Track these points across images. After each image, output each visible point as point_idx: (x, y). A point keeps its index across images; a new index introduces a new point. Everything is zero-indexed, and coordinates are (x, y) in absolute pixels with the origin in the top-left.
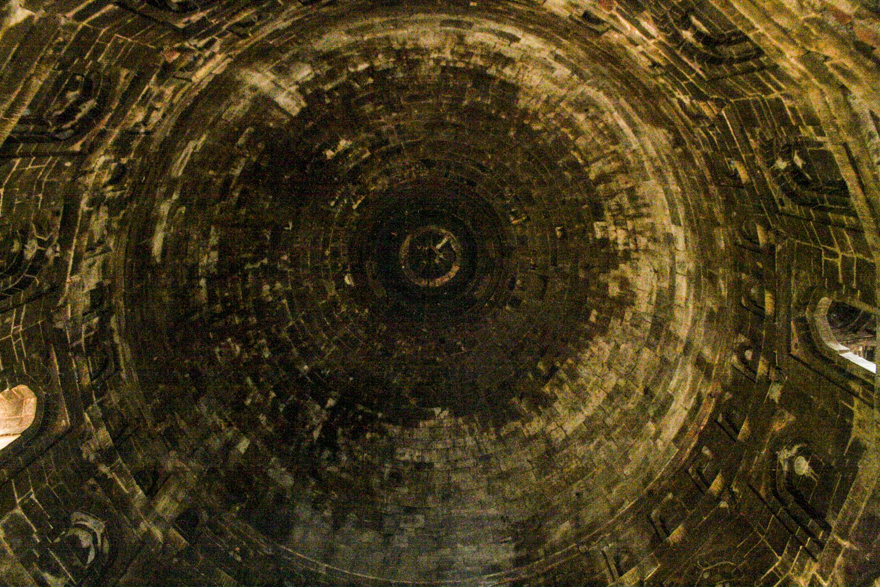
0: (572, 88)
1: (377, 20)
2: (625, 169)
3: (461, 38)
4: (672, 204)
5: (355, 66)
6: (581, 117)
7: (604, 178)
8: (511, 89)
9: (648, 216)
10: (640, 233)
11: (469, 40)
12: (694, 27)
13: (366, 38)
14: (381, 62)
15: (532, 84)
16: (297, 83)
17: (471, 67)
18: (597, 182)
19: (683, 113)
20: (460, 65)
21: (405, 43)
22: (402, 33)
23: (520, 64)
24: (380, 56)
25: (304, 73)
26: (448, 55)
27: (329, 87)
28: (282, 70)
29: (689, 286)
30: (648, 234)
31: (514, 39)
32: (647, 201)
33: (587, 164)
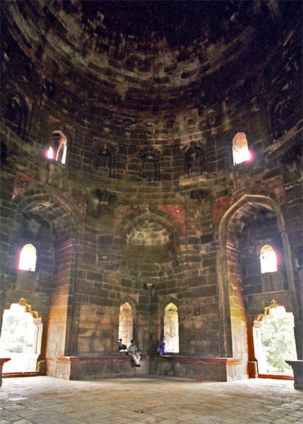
0: (154, 68)
2: (116, 53)
3: (201, 61)
4: (97, 68)
6: (143, 58)
7: (118, 41)
8: (172, 46)
9: (95, 50)
10: (91, 38)
11: (197, 61)
15: (166, 55)
18: (118, 36)
29: (66, 54)
30: (89, 41)
31: (185, 76)
32: (101, 54)
33: (127, 39)
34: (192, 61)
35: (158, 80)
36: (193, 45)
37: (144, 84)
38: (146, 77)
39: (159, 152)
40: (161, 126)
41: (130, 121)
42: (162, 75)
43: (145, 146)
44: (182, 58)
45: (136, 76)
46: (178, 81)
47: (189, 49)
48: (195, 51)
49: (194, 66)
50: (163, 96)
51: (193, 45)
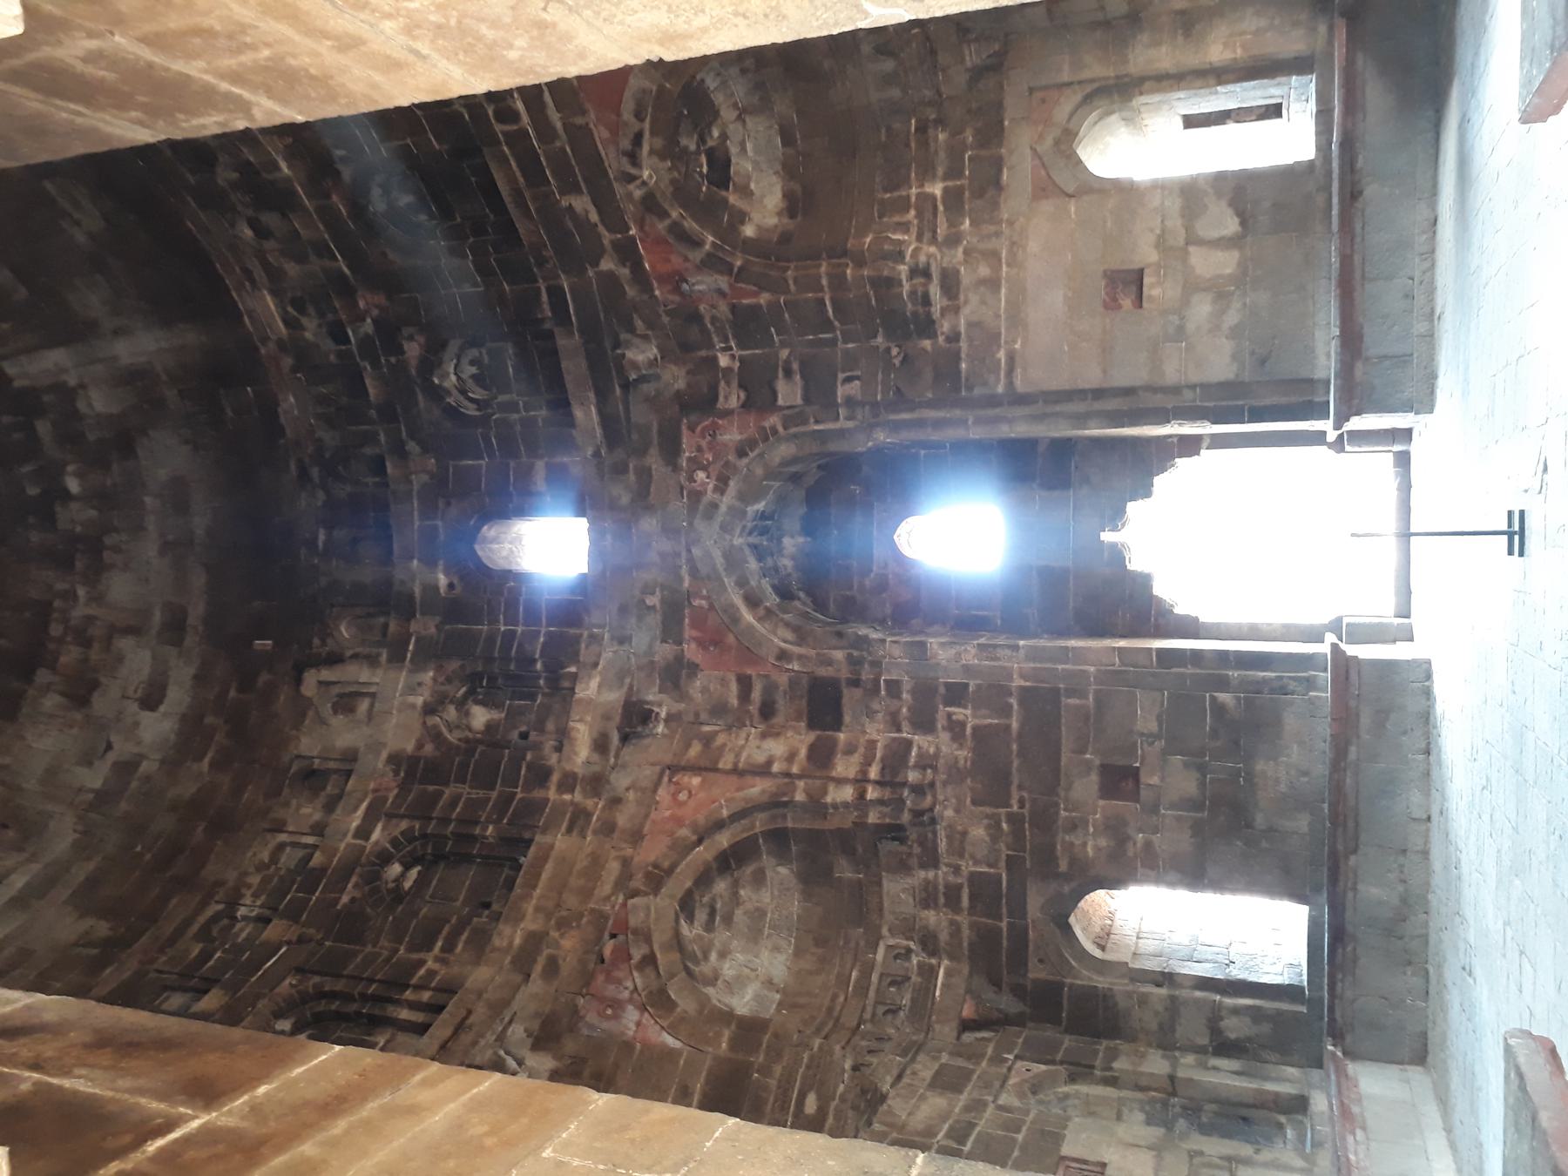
1: (200, 523)
3: (133, 631)
5: (80, 475)
11: (124, 644)
12: (403, 875)
13: (148, 500)
14: (76, 516)
16: (82, 386)
17: (52, 646)
19: (202, 919)
20: (55, 630)
21: (116, 549)
22: (149, 549)
23: (78, 716)
24: (93, 513)
25: (99, 402)
26: (79, 612)
27: (43, 428)
28: (134, 377)
34: (120, 659)
35: (103, 798)
36: (60, 641)
37: (82, 849)
38: (63, 836)
39: (408, 835)
40: (310, 812)
41: (215, 919)
42: (94, 778)
43: (354, 879)
44: (81, 691)
45: (36, 867)
46: (156, 728)
47: (63, 659)
48: (87, 643)
49: (138, 660)
50: (186, 789)
51: (60, 641)
